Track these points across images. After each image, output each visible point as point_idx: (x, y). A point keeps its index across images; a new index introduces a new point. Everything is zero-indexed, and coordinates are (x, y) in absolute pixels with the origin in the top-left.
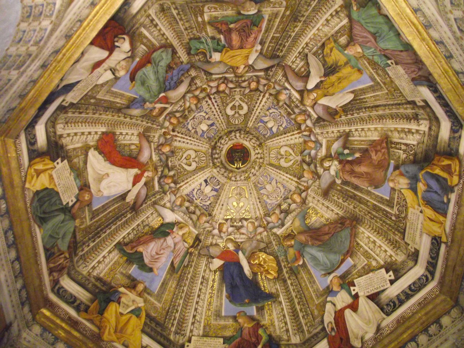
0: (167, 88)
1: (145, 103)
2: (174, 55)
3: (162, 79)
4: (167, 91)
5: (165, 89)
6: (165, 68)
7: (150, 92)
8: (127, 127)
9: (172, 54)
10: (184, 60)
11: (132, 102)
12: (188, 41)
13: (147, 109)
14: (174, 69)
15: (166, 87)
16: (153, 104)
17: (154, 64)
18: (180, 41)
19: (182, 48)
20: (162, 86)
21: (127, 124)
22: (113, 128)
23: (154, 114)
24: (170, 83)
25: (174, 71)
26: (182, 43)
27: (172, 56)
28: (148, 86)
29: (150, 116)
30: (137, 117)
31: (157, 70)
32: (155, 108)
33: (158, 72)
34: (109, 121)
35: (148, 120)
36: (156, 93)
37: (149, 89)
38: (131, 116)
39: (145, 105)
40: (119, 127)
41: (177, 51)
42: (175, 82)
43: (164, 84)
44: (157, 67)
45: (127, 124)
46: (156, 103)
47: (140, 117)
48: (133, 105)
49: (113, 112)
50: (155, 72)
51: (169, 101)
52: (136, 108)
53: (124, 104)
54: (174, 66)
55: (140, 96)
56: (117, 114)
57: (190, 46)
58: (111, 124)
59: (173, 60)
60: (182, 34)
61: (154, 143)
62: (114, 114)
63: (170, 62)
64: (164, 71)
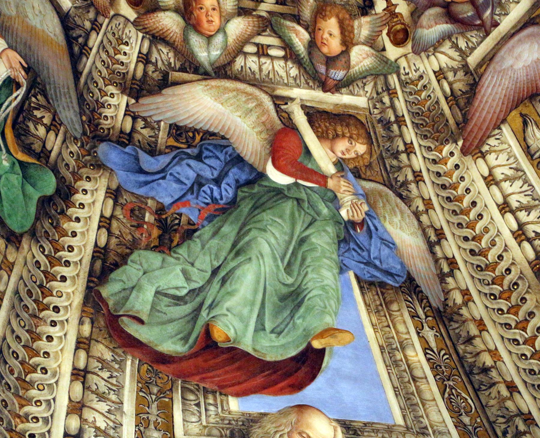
0: (243, 177)
1: (352, 224)
2: (112, 257)
3: (226, 229)
4: (252, 168)
5: (249, 183)
6: (182, 251)
7: (302, 241)
8: (479, 226)
9: (116, 266)
10: (101, 194)
11: (382, 285)
12: (25, 244)
13: (367, 196)
14: (161, 210)
15: (239, 186)
16: (331, 183)
17: (204, 313)
18: (49, 276)
19: (68, 241)
20: (245, 208)
21: (468, 232)
22: (522, 287)
23: (361, 148)
24: (218, 181)
25: (167, 201)
26: (54, 261)
27: (124, 259)
28: (288, 268)
29: (382, 158)
30: (417, 215)
31: (209, 281)
32: (340, 164)
33: (215, 272)
34: (508, 326)
35: (396, 155)
36: (288, 206)
37: (294, 254)
38: (431, 246)
39: (358, 217)
40: (503, 265)
41: (94, 258)
42: (199, 158)
43: (233, 203)
44: (201, 289)
45: (468, 232)
46: (322, 178)
47: (407, 200)
48: (388, 273)
49: (469, 340)
50: (224, 281)
51: (278, 125)
52: (390, 244)
53: (414, 316)
54: (148, 217)
55: (342, 269)
56: (464, 311)
57: (37, 218)
58: (514, 309)
59: (134, 246)
60: (23, 294)
61: (464, 55)
62: (474, 330)
63: (148, 248)
64: (195, 245)
